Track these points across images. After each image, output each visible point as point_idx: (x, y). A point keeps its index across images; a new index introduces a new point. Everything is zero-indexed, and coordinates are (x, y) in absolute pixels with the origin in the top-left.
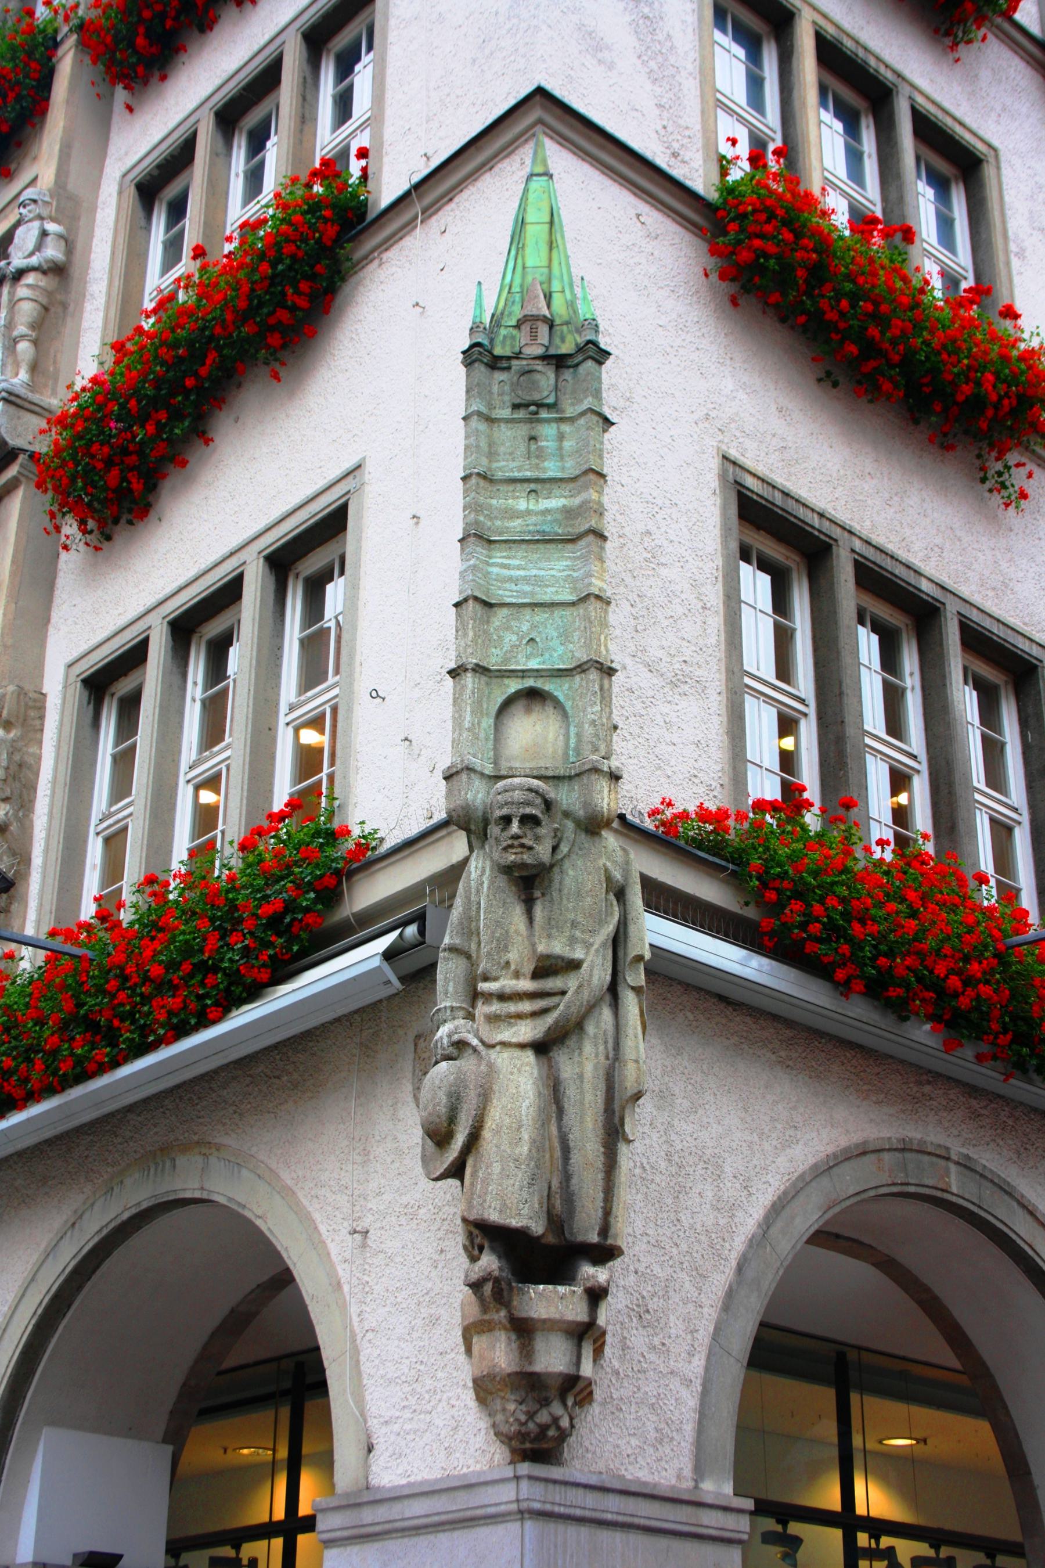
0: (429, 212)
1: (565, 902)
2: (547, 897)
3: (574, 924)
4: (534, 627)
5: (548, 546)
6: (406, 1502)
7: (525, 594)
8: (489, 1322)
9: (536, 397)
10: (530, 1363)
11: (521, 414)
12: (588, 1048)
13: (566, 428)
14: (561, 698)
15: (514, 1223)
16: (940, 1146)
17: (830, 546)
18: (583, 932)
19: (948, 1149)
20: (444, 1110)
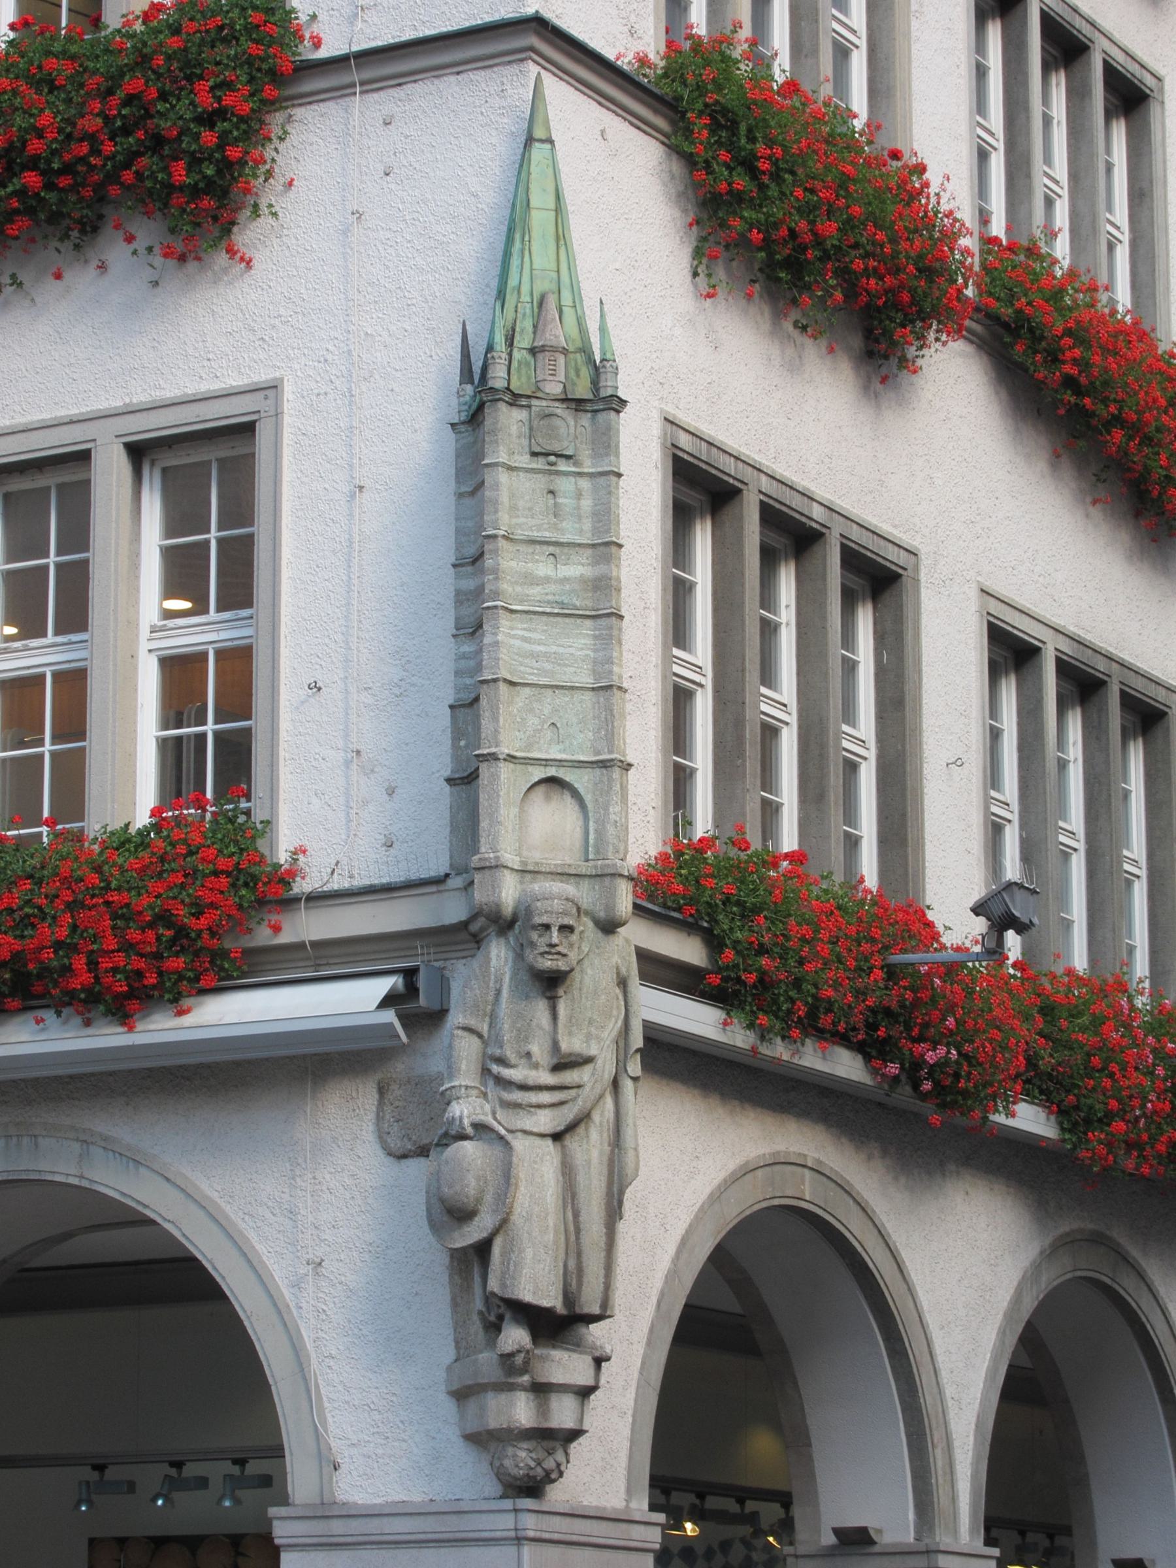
0: (370, 86)
1: (584, 1000)
2: (569, 996)
3: (591, 1022)
4: (555, 711)
5: (567, 620)
6: (385, 1520)
7: (545, 673)
8: (512, 1384)
9: (556, 447)
10: (546, 1420)
11: (539, 464)
12: (594, 1135)
13: (585, 484)
14: (582, 791)
15: (546, 1303)
16: (800, 1154)
17: (739, 491)
18: (597, 1028)
19: (805, 1156)
20: (473, 1192)
